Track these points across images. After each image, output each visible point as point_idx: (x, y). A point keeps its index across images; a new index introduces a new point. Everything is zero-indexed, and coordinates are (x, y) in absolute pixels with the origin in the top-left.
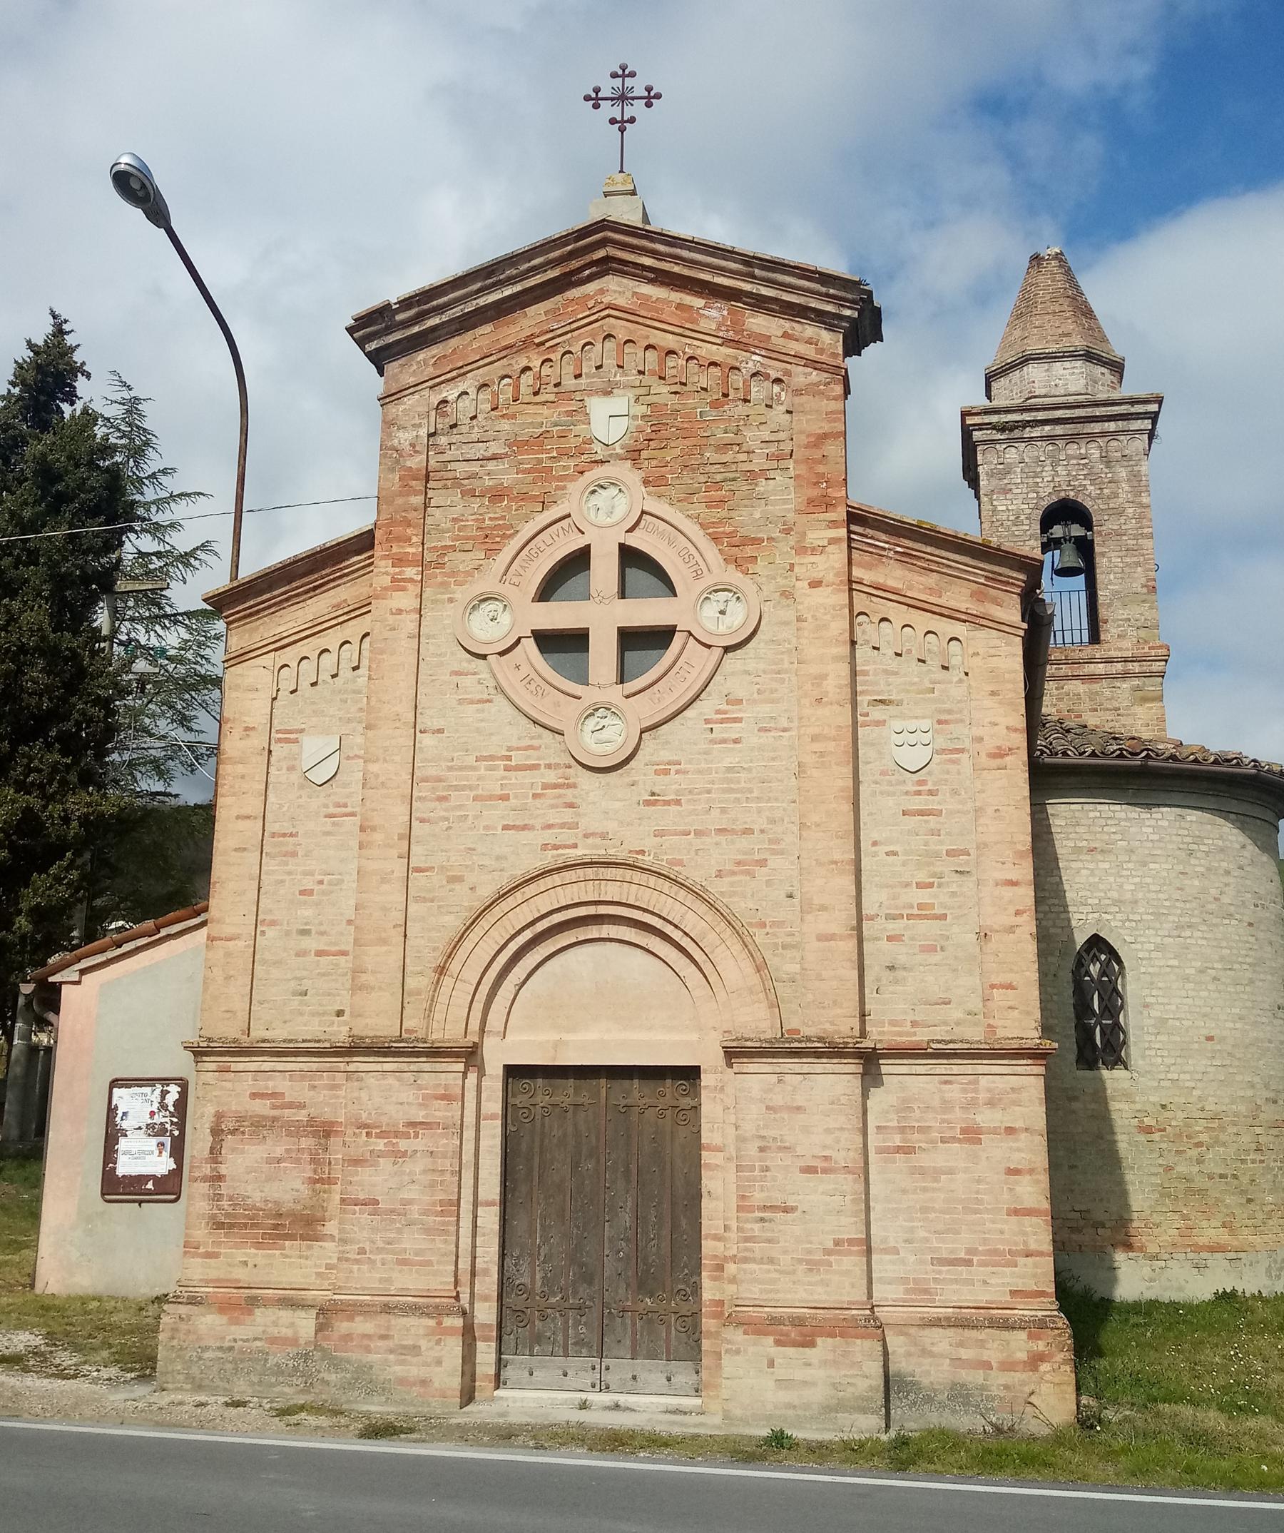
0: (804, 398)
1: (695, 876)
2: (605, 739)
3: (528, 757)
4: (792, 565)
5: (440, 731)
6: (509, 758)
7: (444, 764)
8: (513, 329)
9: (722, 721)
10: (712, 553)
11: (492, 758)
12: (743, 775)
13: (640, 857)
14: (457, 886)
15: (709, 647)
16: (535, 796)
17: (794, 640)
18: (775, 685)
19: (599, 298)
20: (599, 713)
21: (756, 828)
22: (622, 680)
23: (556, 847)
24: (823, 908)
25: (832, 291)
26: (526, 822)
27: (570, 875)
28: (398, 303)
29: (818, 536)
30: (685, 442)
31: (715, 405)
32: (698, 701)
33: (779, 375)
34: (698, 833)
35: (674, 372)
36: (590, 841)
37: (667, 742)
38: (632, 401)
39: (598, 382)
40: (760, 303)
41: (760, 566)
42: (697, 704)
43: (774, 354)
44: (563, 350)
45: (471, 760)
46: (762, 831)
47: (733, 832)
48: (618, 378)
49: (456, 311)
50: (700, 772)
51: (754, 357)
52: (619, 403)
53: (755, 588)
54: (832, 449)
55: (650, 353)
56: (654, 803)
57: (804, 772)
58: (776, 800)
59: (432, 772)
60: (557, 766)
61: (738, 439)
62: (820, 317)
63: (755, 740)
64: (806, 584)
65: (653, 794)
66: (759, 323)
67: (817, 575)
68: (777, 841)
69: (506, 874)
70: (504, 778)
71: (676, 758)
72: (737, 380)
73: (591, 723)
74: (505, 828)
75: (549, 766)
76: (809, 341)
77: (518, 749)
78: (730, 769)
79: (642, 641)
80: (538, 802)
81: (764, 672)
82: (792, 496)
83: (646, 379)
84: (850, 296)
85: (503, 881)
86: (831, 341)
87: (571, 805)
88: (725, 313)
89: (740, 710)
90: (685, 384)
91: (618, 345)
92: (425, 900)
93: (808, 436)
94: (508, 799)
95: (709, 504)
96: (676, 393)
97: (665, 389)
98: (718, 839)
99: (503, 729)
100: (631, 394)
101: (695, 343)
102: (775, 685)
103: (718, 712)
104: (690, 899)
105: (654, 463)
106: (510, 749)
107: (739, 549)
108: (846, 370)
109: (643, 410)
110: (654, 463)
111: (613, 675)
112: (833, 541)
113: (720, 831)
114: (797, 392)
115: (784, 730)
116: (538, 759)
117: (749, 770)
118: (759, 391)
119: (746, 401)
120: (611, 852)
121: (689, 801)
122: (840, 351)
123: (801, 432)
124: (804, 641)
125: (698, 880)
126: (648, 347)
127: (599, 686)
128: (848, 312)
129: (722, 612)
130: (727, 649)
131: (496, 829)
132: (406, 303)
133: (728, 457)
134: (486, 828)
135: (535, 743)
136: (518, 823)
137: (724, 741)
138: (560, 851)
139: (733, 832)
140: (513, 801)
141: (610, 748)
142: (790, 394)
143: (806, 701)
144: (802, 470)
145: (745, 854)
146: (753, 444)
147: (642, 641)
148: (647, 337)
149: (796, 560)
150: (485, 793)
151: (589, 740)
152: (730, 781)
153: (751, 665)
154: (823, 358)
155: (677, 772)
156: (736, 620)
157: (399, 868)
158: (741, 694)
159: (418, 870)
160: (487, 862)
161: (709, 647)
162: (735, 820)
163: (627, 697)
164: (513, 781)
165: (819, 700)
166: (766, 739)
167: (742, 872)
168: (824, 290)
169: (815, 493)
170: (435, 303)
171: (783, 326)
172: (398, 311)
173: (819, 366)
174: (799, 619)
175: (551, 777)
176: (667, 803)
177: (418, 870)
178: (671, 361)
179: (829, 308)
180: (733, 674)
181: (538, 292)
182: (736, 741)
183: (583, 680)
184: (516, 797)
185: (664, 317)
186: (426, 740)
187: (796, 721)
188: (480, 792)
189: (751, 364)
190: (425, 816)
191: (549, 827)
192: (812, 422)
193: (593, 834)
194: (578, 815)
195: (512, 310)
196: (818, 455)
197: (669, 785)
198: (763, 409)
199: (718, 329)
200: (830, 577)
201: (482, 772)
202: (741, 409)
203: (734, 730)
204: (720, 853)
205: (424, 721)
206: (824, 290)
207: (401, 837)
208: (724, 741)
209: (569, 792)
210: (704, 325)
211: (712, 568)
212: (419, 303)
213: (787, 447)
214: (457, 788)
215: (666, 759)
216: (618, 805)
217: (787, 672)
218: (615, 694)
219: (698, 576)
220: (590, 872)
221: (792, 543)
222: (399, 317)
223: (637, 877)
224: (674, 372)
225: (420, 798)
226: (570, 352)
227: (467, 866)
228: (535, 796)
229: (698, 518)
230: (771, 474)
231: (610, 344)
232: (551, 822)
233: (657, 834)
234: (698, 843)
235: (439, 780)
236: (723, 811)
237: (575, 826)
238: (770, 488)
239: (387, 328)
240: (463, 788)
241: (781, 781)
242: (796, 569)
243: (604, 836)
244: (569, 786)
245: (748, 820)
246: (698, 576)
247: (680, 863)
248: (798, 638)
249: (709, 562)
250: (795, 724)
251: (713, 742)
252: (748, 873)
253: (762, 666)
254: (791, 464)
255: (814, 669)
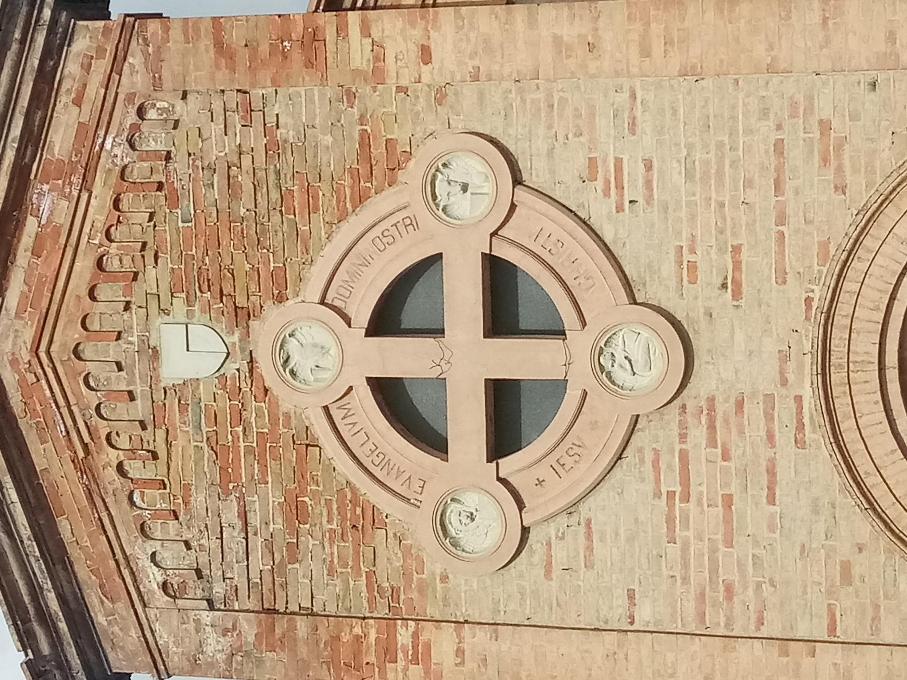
0: (166, 74)
1: (843, 226)
2: (643, 356)
3: (670, 467)
4: (399, 89)
5: (631, 595)
6: (671, 495)
7: (679, 588)
8: (65, 487)
9: (620, 187)
10: (380, 204)
11: (670, 520)
12: (698, 155)
13: (815, 304)
14: (856, 571)
15: (513, 207)
16: (726, 457)
17: (505, 85)
18: (569, 112)
19: (23, 367)
20: (605, 361)
21: (774, 136)
22: (560, 333)
23: (801, 426)
24: (891, 37)
25: (17, 35)
26: (763, 469)
27: (842, 405)
28: (25, 649)
29: (358, 52)
30: (224, 243)
31: (173, 201)
32: (592, 222)
33: (133, 111)
34: (781, 220)
35: (127, 260)
36: (791, 377)
37: (650, 266)
38: (166, 319)
39: (140, 368)
40: (34, 138)
41: (400, 134)
42: (594, 222)
43: (104, 117)
44: (95, 418)
45: (674, 551)
46: (779, 127)
47: (779, 170)
48: (134, 339)
49: (38, 568)
50: (692, 218)
51: (108, 146)
52: (169, 336)
53: (430, 142)
54: (236, 37)
55: (100, 294)
56: (737, 284)
57: (693, 67)
58: (734, 107)
59: (690, 607)
60: (683, 425)
61: (222, 167)
62: (54, 52)
63: (647, 140)
64: (425, 69)
65: (724, 286)
66: (60, 140)
67: (414, 52)
68: (794, 105)
69: (839, 499)
70: (700, 503)
71: (672, 253)
72: (139, 171)
73: (621, 375)
74: (771, 500)
75: (683, 437)
76: (87, 68)
77: (658, 481)
78: (689, 175)
79: (505, 303)
80: (734, 453)
81: (550, 127)
82: (302, 90)
83: (137, 299)
84: (24, 10)
85: (849, 504)
86: (86, 37)
87: (740, 405)
88: (46, 187)
89: (605, 161)
90: (144, 244)
91: (88, 339)
92: (876, 619)
93: (217, 66)
94: (730, 496)
95: (311, 208)
96: (156, 257)
97: (151, 272)
98: (789, 193)
99: (627, 503)
100: (157, 321)
101: (86, 229)
102: (569, 112)
103: (607, 193)
104: (877, 231)
105: (253, 287)
106: (658, 494)
107: (376, 164)
108: (127, 15)
109: (179, 304)
110: (253, 287)
111: (553, 344)
112: (366, 31)
113: (778, 187)
114: (157, 84)
115: (633, 96)
116: (672, 452)
117: (690, 147)
118: (155, 140)
119: (168, 157)
120: (808, 347)
121: (734, 234)
122: (101, 24)
123: (213, 79)
124: (507, 70)
125: (849, 220)
126: (92, 296)
127: (567, 364)
128: (47, 13)
129: (465, 188)
130: (517, 181)
131: (772, 516)
132: (26, 639)
133: (245, 180)
134: (771, 528)
135: (649, 457)
136: (765, 483)
137: (648, 183)
138: (806, 421)
139: (779, 170)
140: (733, 490)
141: (657, 347)
142: (159, 95)
143: (592, 67)
144: (265, 76)
145: (811, 152)
146: (229, 143)
147: (505, 303)
148: (78, 297)
149: (392, 82)
150: (722, 529)
151: (645, 379)
152: (706, 176)
153: (541, 145)
154: (110, 48)
155: (692, 251)
156: (476, 169)
157: (829, 656)
158: (581, 161)
159: (832, 629)
160: (821, 527)
161: (513, 207)
162: (763, 168)
163: (584, 324)
164: (704, 488)
165: (591, 47)
166: (645, 122)
167: (839, 156)
168: (15, 47)
169: (297, 56)
170: (26, 599)
171: (66, 106)
172: (37, 651)
173: (121, 54)
174: (476, 78)
175: (698, 434)
176: (737, 265)
177: (832, 629)
178: (112, 264)
179: (40, 39)
180: (552, 172)
181: (15, 453)
182: (649, 166)
183: (558, 388)
184: (727, 485)
185: (51, 274)
186: (645, 615)
187: (621, 80)
188: (720, 537)
189: (118, 151)
190: (754, 618)
191: (770, 437)
192: (200, 66)
193: (782, 373)
194: (754, 394)
195: (38, 489)
196: (243, 55)
197: (712, 263)
198: (180, 134)
199: (68, 197)
200: (416, 33)
201: (691, 534)
202: (180, 164)
203: (633, 171)
204: (810, 188)
205: (616, 615)
206: (15, 47)
207: (785, 653)
208: (648, 183)
209: (720, 408)
210: (62, 219)
211: (402, 202)
212: (26, 621)
213: (233, 98)
214: (714, 570)
215: (673, 267)
216: (739, 337)
217: (550, 95)
218: (580, 342)
219: (413, 223)
220: (837, 377)
221: (368, 89)
222: (45, 649)
223: (844, 308)
224: (127, 260)
225: (727, 626)
226: (98, 408)
227: (828, 556)
228: (726, 457)
229: (330, 224)
230: (271, 121)
231: (88, 351)
232: (763, 433)
233: (782, 279)
234: (795, 220)
235: (702, 596)
236: (749, 184)
237: (769, 400)
238: (290, 121)
239: (60, 667)
240: (713, 561)
241: (706, 101)
242: (404, 82)
243: (784, 357)
244: (712, 408)
245: (762, 147)
246: (413, 223)
247: (824, 246)
248: (502, 79)
249: (390, 209)
250: (626, 83)
251: (649, 200)
252: (839, 148)
253: (541, 131)
254: (257, 93)
255: (547, 55)
